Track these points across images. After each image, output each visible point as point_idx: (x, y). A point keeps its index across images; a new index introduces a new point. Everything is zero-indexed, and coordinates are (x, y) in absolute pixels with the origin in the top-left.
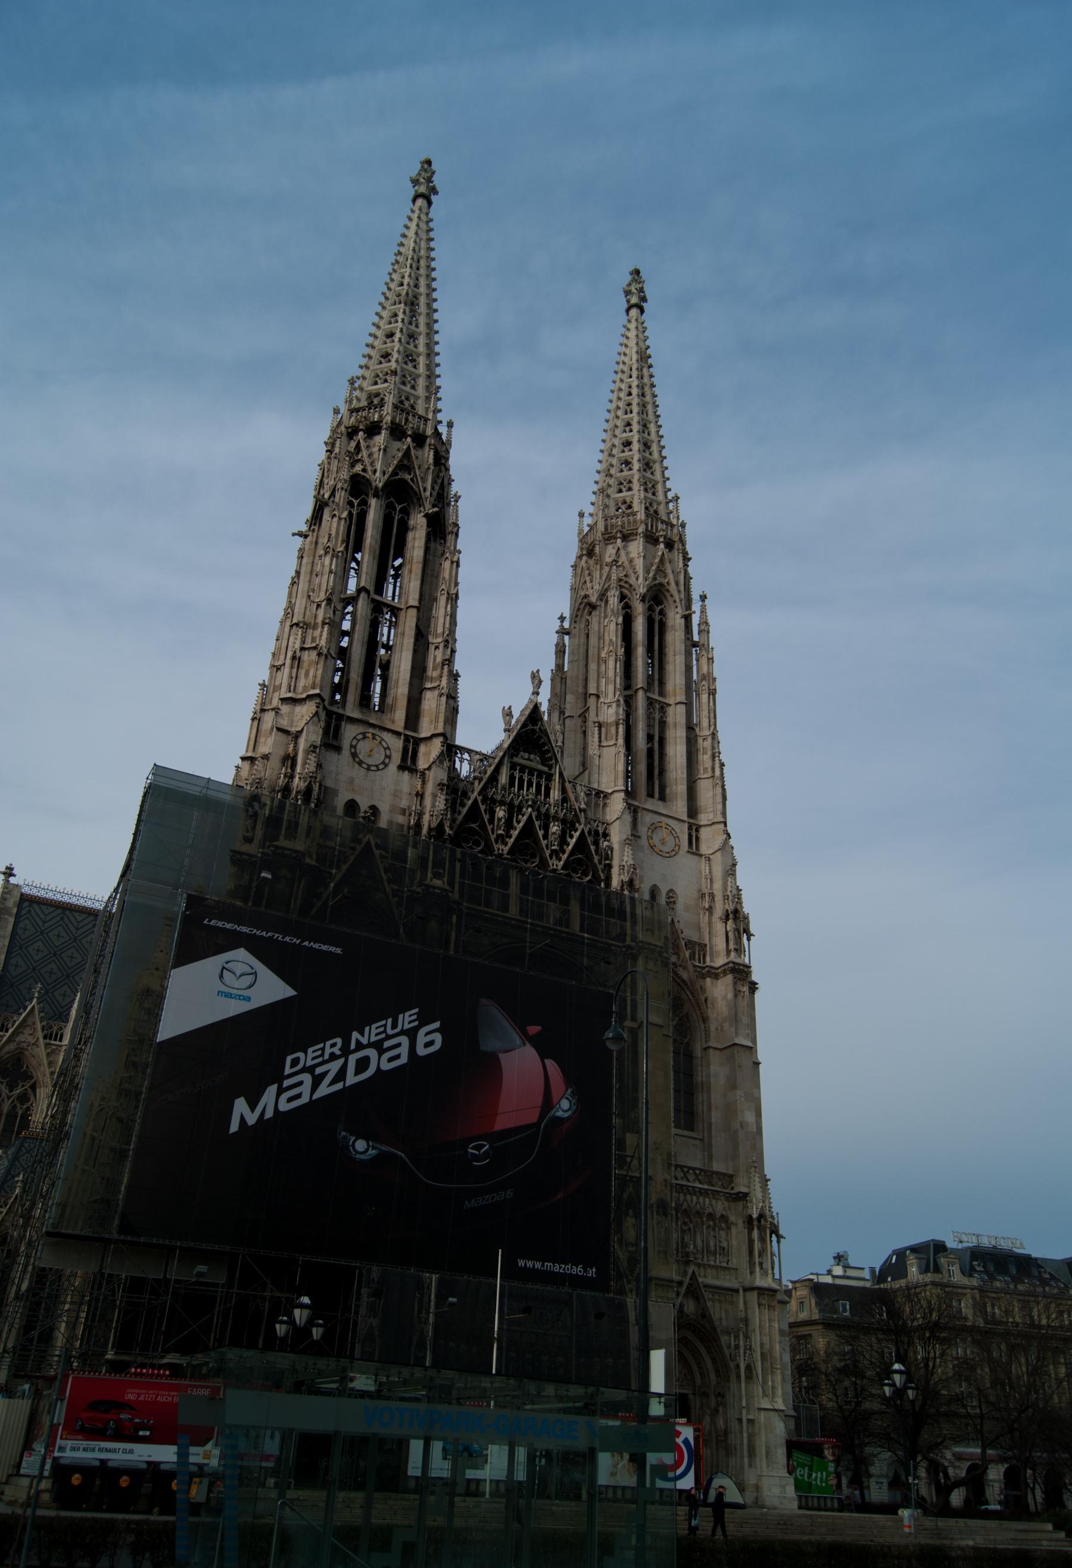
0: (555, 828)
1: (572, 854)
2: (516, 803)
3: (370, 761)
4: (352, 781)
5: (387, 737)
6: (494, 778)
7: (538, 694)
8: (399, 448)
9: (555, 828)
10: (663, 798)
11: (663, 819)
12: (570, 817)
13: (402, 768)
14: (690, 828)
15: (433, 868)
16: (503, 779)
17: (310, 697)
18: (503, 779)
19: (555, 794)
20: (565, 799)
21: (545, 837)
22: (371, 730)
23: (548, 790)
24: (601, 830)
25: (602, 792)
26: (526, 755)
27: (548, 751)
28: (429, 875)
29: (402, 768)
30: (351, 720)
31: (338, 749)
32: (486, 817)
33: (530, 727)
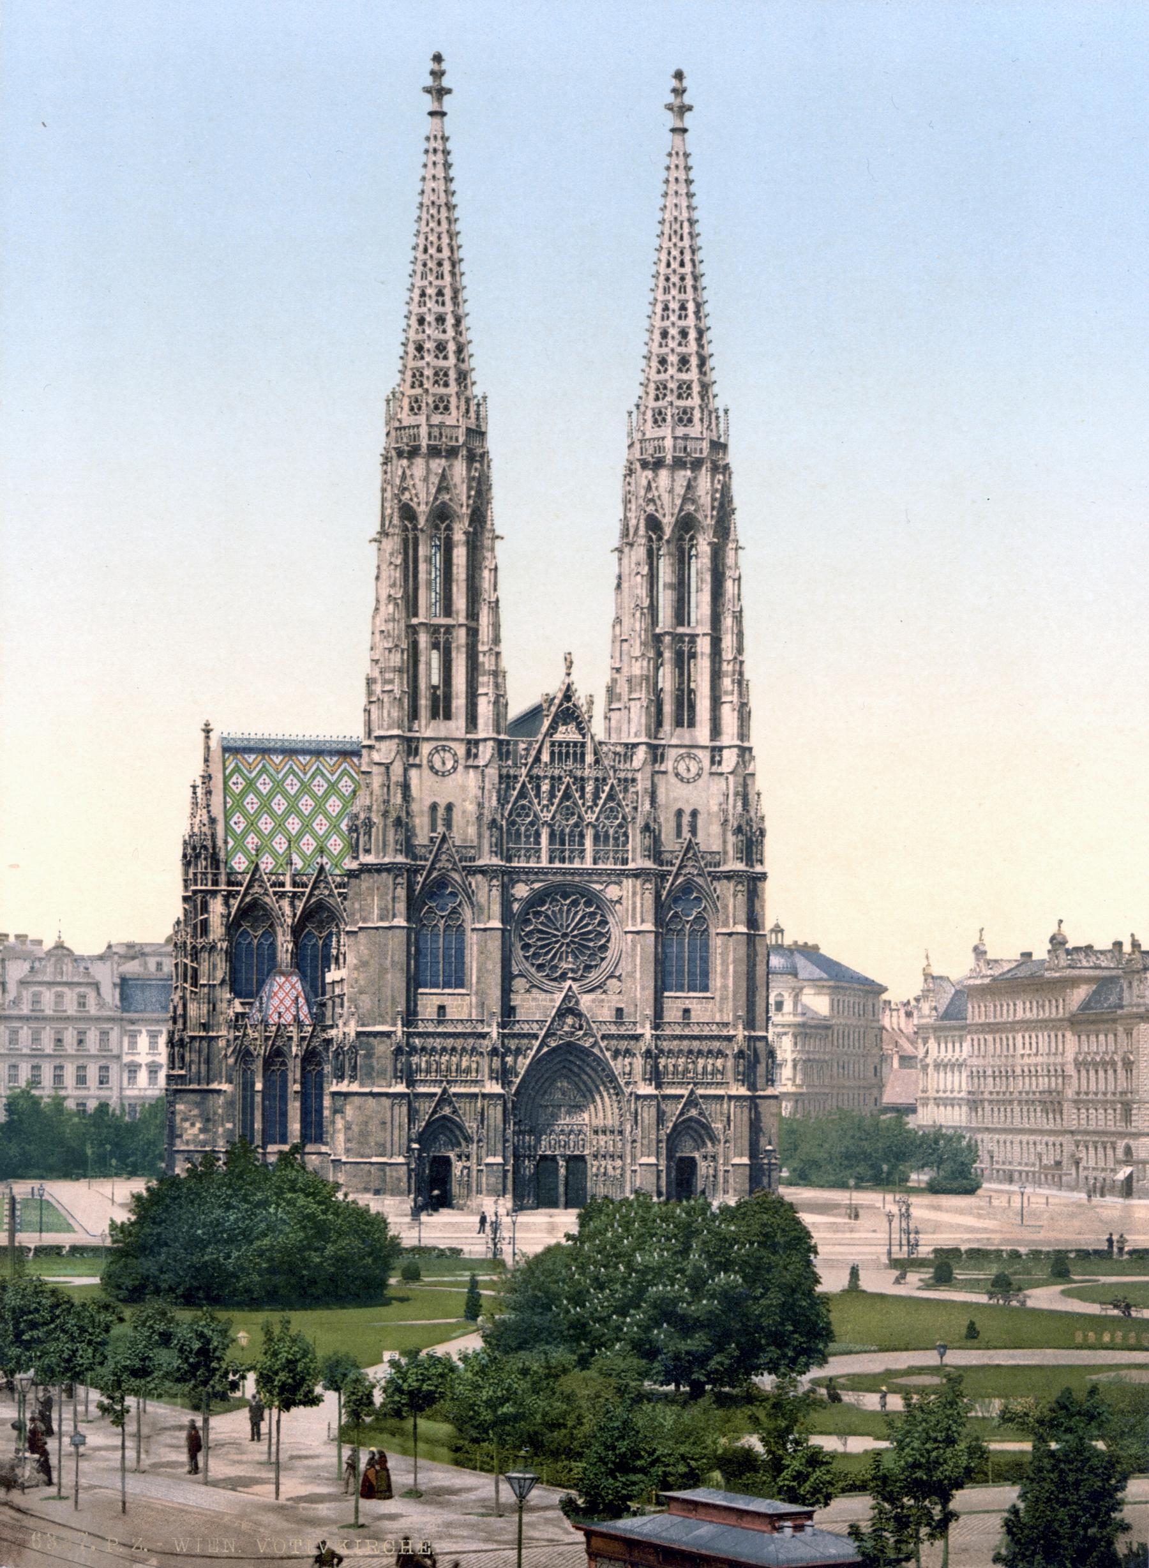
0: (589, 788)
1: (605, 804)
6: (537, 759)
8: (438, 465)
9: (589, 788)
12: (600, 775)
16: (545, 757)
17: (391, 737)
18: (545, 757)
19: (589, 758)
23: (583, 755)
26: (562, 729)
29: (467, 767)
31: (419, 766)
33: (566, 705)
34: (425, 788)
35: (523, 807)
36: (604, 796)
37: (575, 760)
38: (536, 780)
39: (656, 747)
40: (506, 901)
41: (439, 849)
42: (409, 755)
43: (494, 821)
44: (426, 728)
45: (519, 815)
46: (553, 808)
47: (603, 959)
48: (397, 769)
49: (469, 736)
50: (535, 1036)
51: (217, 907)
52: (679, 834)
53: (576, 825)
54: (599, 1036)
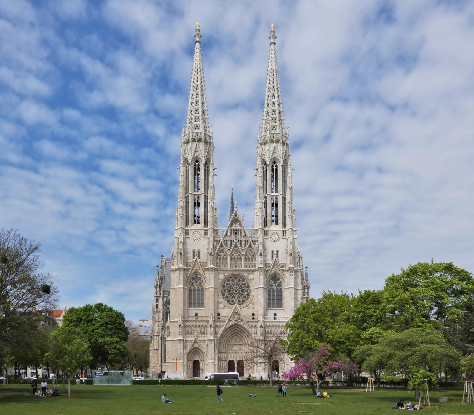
1: (248, 248)
5: (200, 231)
6: (226, 235)
10: (277, 224)
16: (229, 234)
19: (243, 234)
20: (245, 235)
21: (241, 246)
23: (241, 233)
24: (256, 240)
34: (192, 246)
35: (222, 250)
39: (265, 231)
40: (216, 279)
41: (195, 263)
42: (186, 234)
43: (211, 253)
44: (192, 227)
45: (220, 252)
47: (248, 298)
48: (181, 239)
49: (205, 228)
50: (225, 322)
51: (161, 300)
52: (272, 259)
53: (239, 255)
54: (246, 321)
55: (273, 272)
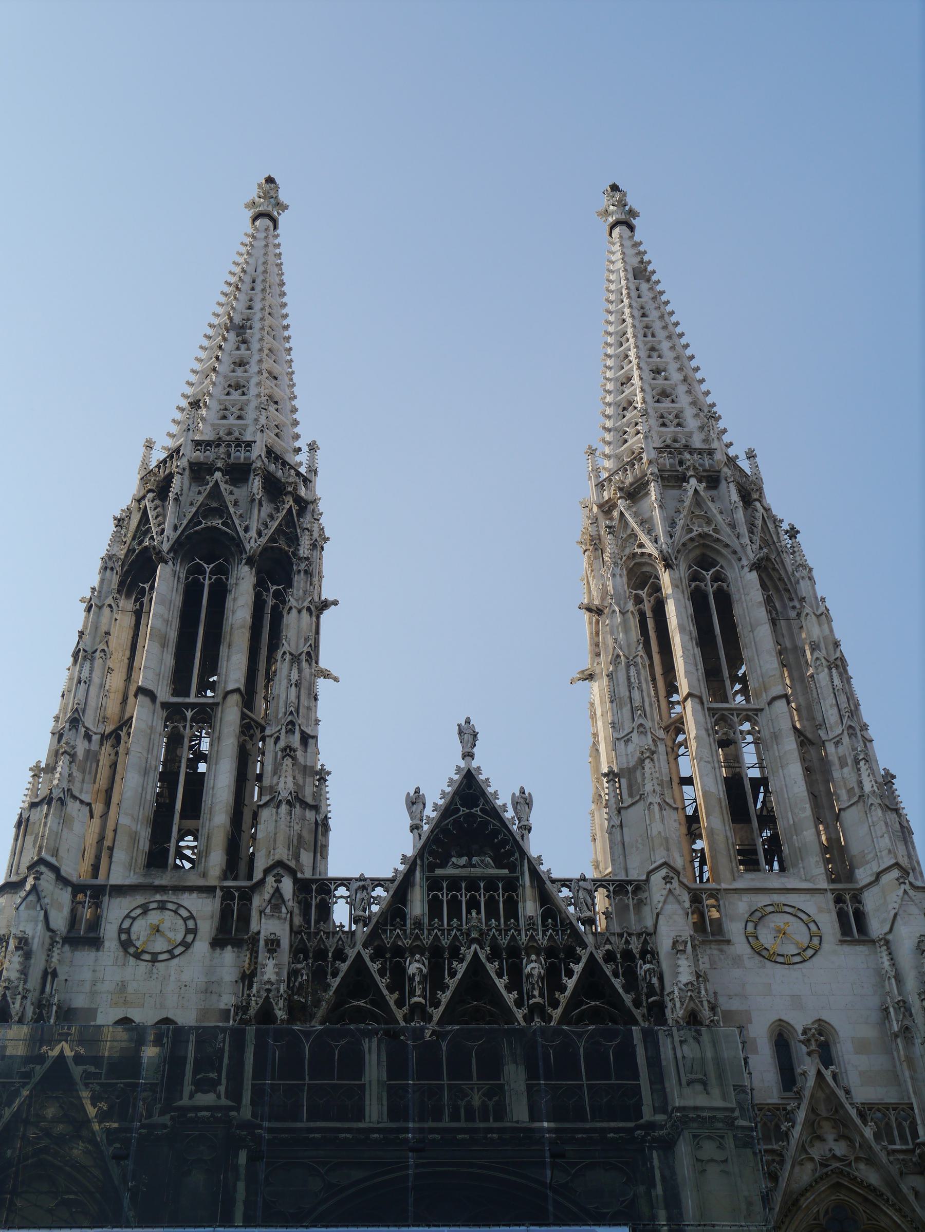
0: (533, 967)
1: (574, 1001)
2: (445, 942)
3: (159, 945)
4: (122, 987)
7: (472, 756)
9: (533, 967)
11: (777, 898)
12: (561, 939)
13: (218, 943)
14: (839, 900)
15: (196, 1072)
16: (417, 906)
18: (417, 906)
19: (530, 908)
22: (158, 897)
24: (635, 946)
25: (629, 882)
27: (504, 842)
28: (188, 1088)
29: (218, 943)
30: (120, 890)
31: (94, 942)
32: (382, 983)
33: (463, 810)
36: (571, 983)
37: (492, 912)
38: (392, 962)
46: (437, 1013)
55: (805, 1175)
